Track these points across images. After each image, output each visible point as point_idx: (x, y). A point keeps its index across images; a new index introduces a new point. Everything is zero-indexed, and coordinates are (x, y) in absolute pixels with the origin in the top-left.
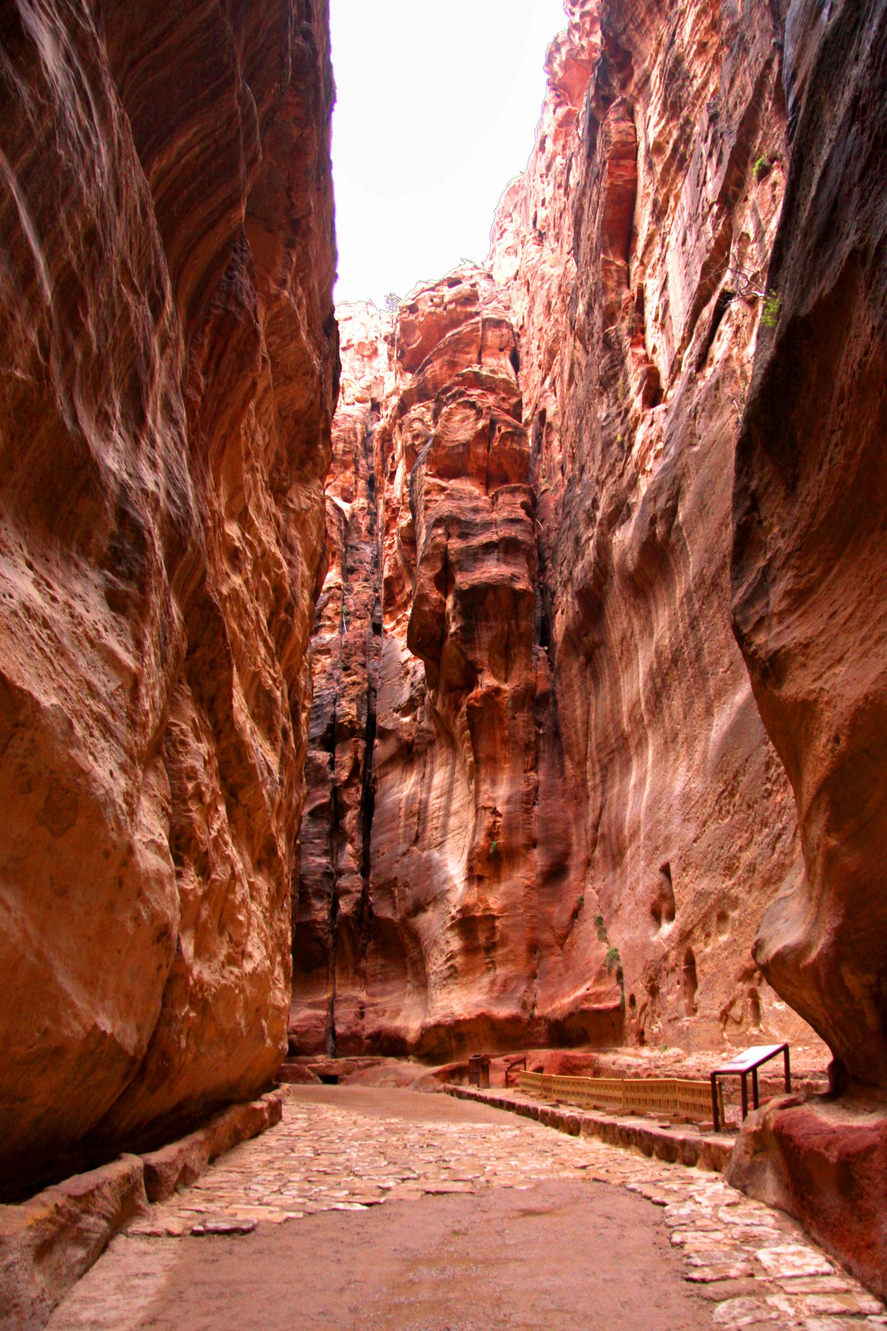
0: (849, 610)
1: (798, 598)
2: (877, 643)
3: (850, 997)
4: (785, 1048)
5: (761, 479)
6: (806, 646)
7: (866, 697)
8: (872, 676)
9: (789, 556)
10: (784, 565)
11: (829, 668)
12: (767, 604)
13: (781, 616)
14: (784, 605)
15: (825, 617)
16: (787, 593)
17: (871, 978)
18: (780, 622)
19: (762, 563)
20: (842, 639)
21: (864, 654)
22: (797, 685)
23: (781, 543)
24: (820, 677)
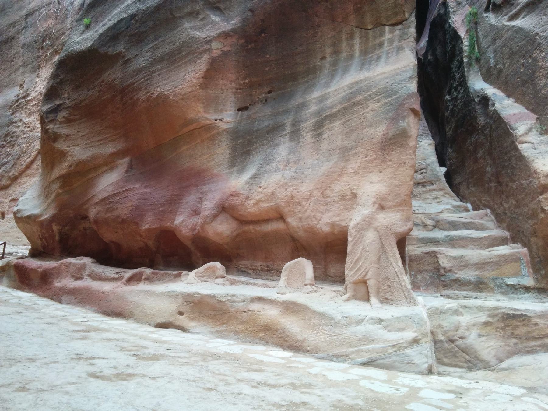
0: (84, 134)
1: (68, 121)
2: (91, 147)
3: (53, 231)
4: (5, 243)
5: (66, 77)
6: (67, 136)
7: (83, 160)
8: (87, 155)
9: (69, 107)
10: (66, 108)
11: (73, 146)
12: (56, 116)
13: (61, 123)
14: (63, 120)
15: (76, 131)
16: (64, 117)
17: (60, 227)
18: (60, 124)
19: (58, 102)
20: (79, 140)
21: (86, 148)
22: (61, 145)
23: (67, 101)
24: (70, 147)
